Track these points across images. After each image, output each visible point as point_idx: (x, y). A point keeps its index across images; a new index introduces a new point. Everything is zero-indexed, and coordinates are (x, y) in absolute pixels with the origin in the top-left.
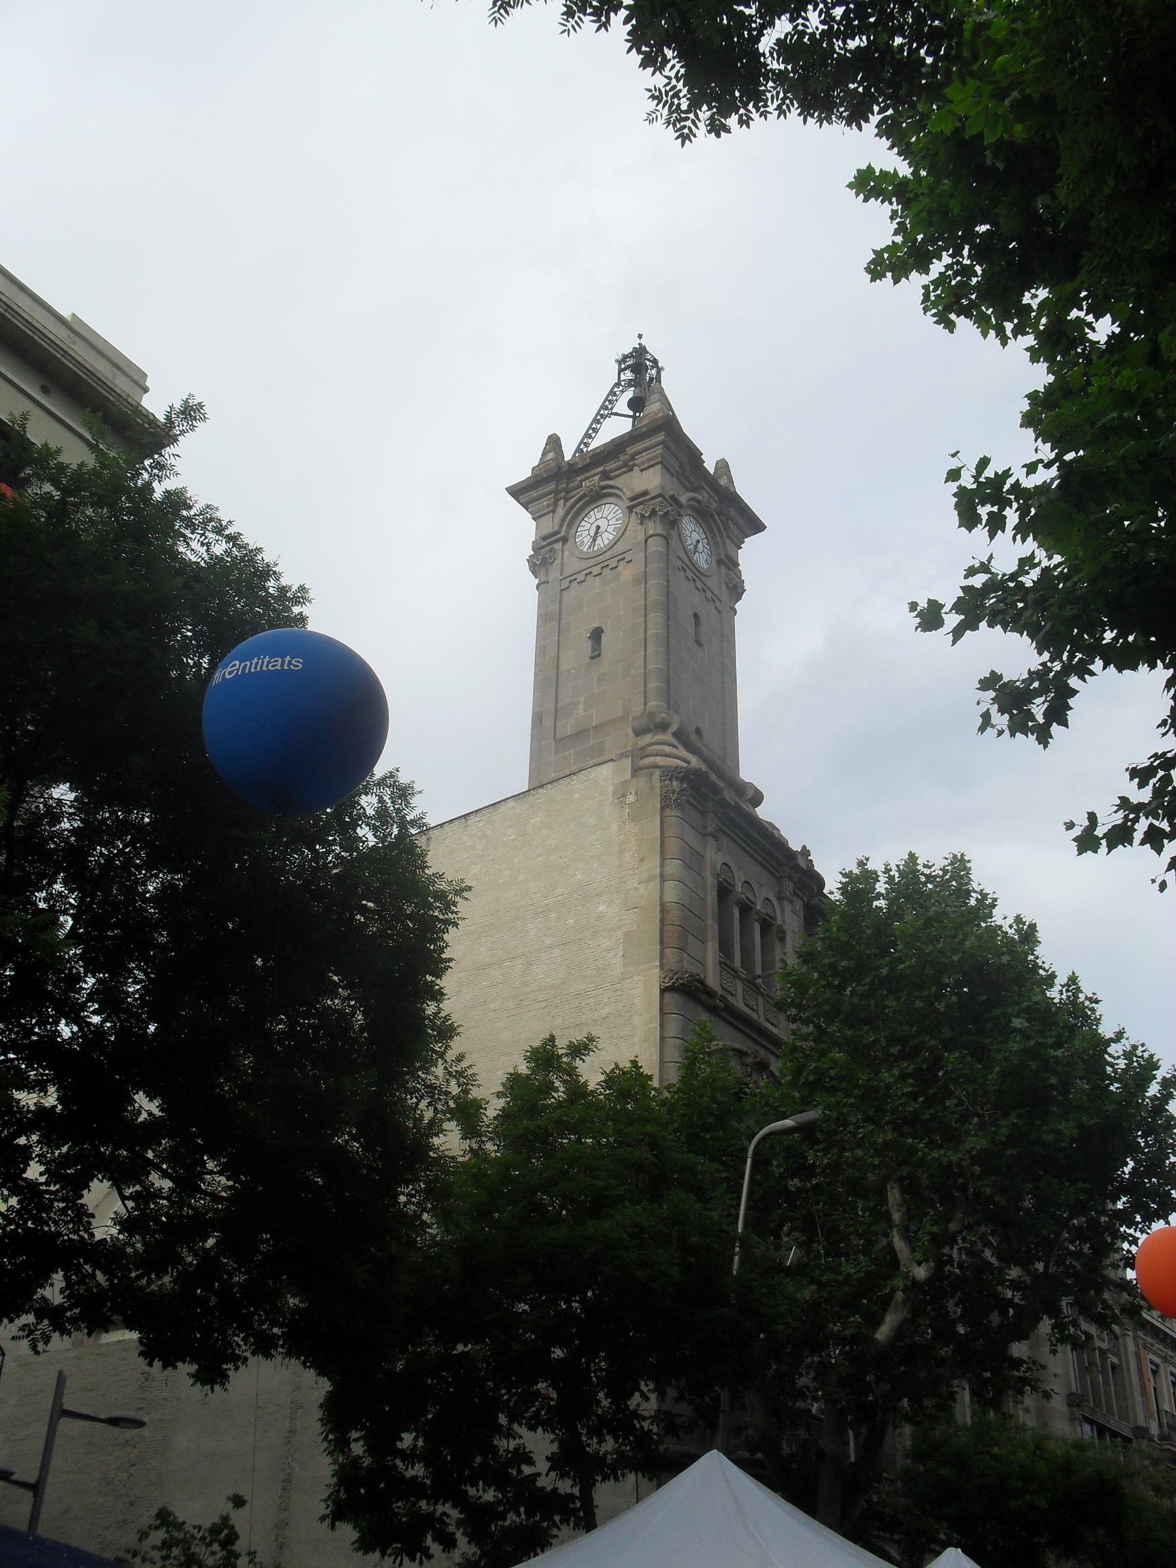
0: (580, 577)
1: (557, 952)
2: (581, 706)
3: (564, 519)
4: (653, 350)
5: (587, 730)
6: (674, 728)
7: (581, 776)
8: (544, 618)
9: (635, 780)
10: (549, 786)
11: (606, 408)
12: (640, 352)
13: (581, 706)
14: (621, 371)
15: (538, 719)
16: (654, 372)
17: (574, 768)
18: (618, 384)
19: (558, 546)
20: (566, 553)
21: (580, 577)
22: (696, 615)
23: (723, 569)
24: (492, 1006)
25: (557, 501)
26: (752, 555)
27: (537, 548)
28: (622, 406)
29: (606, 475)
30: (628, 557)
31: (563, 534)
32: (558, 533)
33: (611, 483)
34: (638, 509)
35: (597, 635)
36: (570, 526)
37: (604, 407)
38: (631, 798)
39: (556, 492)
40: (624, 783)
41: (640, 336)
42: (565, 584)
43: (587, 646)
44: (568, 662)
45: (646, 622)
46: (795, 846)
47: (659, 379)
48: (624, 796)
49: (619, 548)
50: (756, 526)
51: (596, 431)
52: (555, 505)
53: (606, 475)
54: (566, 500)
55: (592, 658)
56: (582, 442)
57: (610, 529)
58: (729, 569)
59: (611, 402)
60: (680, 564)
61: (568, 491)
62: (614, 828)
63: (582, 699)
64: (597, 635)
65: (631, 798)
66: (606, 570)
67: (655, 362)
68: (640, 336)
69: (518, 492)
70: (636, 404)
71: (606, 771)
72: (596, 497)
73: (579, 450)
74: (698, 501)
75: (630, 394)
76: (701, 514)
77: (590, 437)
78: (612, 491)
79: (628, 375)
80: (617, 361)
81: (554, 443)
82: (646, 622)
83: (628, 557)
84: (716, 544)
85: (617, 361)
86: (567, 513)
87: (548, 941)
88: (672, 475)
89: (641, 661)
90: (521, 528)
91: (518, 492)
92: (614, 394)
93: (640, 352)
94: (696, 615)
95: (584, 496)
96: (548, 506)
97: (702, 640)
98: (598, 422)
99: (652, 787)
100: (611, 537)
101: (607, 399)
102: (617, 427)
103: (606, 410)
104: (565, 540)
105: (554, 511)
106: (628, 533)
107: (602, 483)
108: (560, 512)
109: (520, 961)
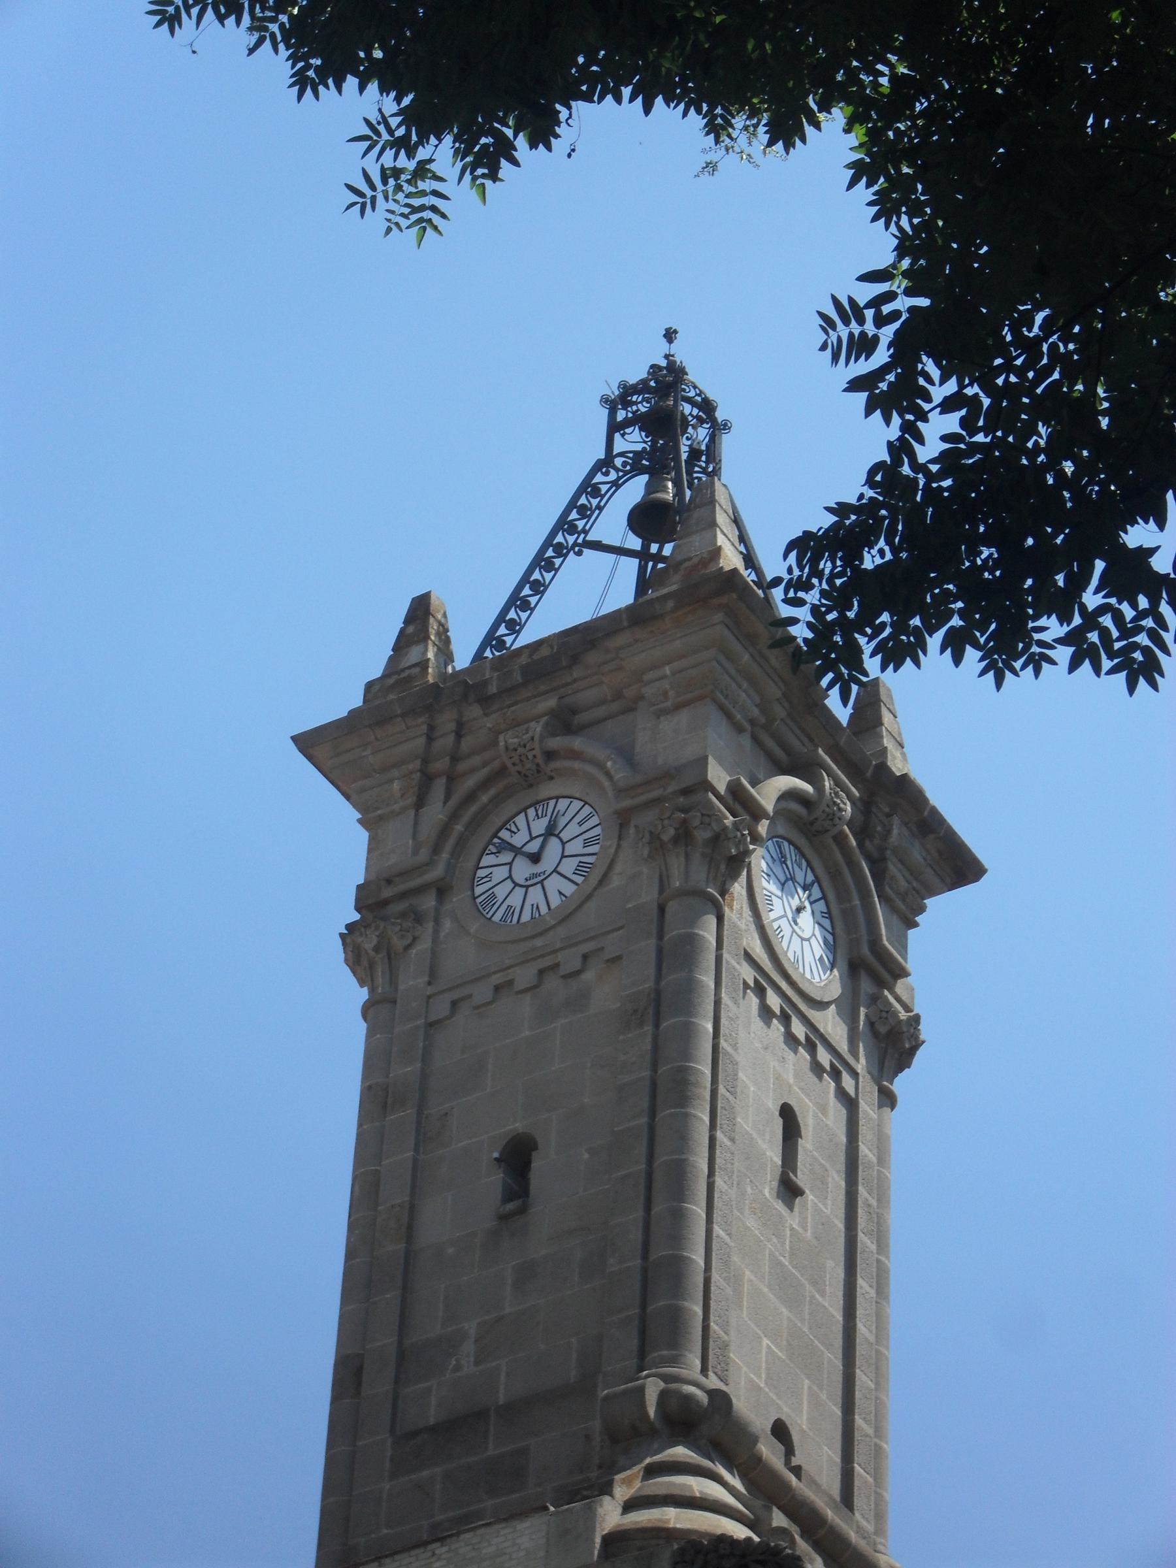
3: (444, 831)
4: (702, 375)
5: (481, 1415)
8: (378, 1099)
11: (572, 529)
12: (668, 379)
13: (469, 1347)
14: (615, 427)
15: (350, 1375)
16: (702, 433)
18: (605, 464)
20: (447, 924)
22: (787, 1113)
28: (612, 523)
31: (437, 872)
33: (577, 743)
34: (647, 818)
35: (518, 1157)
36: (459, 850)
37: (563, 524)
41: (670, 335)
43: (494, 1181)
44: (440, 1222)
45: (652, 1129)
47: (712, 452)
50: (960, 867)
51: (539, 588)
55: (504, 1218)
56: (501, 619)
57: (568, 867)
59: (584, 512)
63: (471, 1327)
64: (518, 1157)
66: (552, 983)
67: (707, 407)
68: (670, 335)
70: (649, 519)
73: (491, 640)
75: (635, 490)
77: (525, 606)
78: (576, 765)
79: (633, 441)
80: (605, 400)
82: (652, 1129)
85: (605, 400)
86: (454, 817)
88: (739, 729)
89: (636, 1236)
92: (596, 492)
93: (668, 379)
94: (787, 1113)
97: (802, 1178)
98: (549, 566)
101: (572, 504)
102: (594, 587)
103: (568, 535)
104: (442, 890)
107: (555, 743)
108: (436, 812)
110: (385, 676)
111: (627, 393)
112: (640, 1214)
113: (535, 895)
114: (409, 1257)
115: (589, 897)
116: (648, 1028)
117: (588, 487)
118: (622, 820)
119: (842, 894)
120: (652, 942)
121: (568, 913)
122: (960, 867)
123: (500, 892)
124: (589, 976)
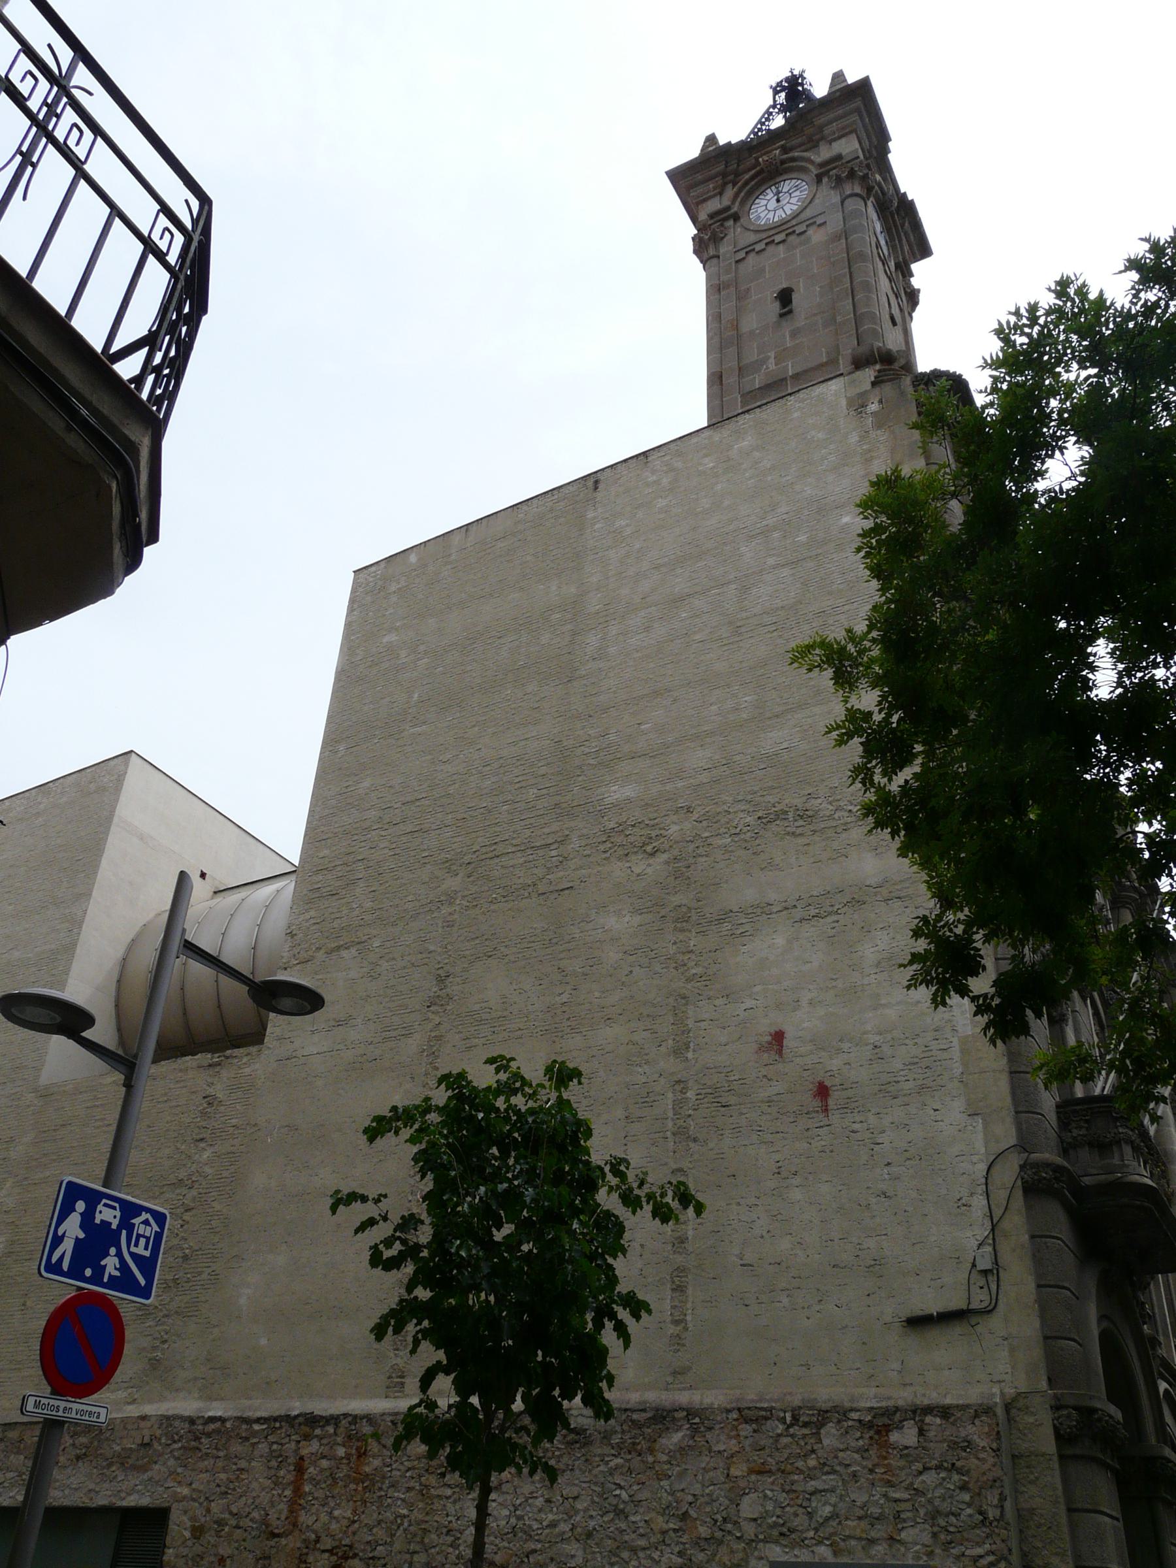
1: (786, 572)
2: (772, 360)
5: (786, 378)
7: (801, 395)
9: (877, 390)
10: (758, 410)
17: (790, 391)
18: (774, 106)
19: (731, 222)
24: (697, 637)
25: (724, 185)
29: (785, 150)
30: (819, 221)
32: (728, 208)
35: (785, 297)
36: (743, 203)
38: (874, 407)
39: (724, 175)
40: (862, 395)
42: (742, 254)
44: (750, 323)
45: (851, 273)
48: (864, 406)
49: (808, 213)
53: (785, 150)
54: (734, 186)
55: (781, 315)
58: (904, 276)
61: (737, 174)
62: (854, 438)
63: (772, 354)
64: (785, 297)
65: (874, 407)
71: (835, 386)
87: (771, 561)
95: (761, 171)
96: (715, 189)
99: (903, 393)
100: (795, 207)
105: (721, 194)
106: (817, 201)
109: (734, 586)
110: (701, 155)
111: (779, 84)
112: (851, 300)
113: (780, 213)
114: (739, 336)
115: (805, 208)
116: (844, 241)
120: (840, 214)
121: (796, 215)
123: (762, 215)
124: (810, 232)
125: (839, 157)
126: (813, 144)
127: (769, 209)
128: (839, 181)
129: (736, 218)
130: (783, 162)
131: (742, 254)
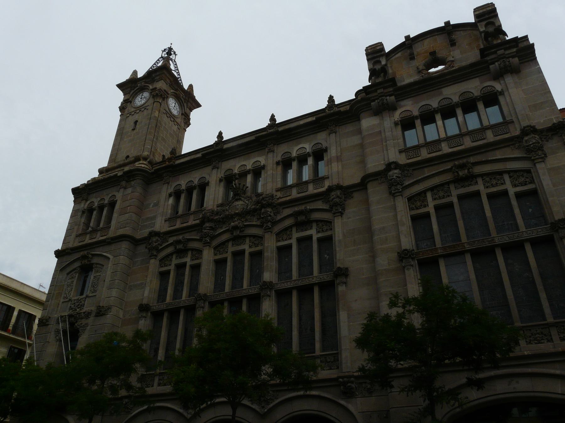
0: (133, 113)
4: (175, 49)
6: (148, 160)
12: (170, 49)
21: (133, 113)
23: (183, 117)
26: (194, 115)
27: (122, 104)
36: (133, 98)
42: (128, 115)
46: (96, 174)
49: (146, 104)
50: (198, 105)
52: (130, 91)
60: (165, 112)
67: (175, 53)
69: (120, 86)
72: (142, 90)
74: (176, 94)
76: (177, 98)
81: (135, 72)
83: (147, 108)
84: (182, 109)
90: (120, 96)
91: (120, 86)
93: (170, 49)
105: (129, 93)
111: (165, 50)
117: (158, 60)
118: (151, 93)
119: (181, 106)
122: (198, 105)
125: (156, 88)
126: (153, 81)
127: (139, 101)
128: (154, 97)
129: (131, 102)
130: (145, 86)
131: (128, 115)
